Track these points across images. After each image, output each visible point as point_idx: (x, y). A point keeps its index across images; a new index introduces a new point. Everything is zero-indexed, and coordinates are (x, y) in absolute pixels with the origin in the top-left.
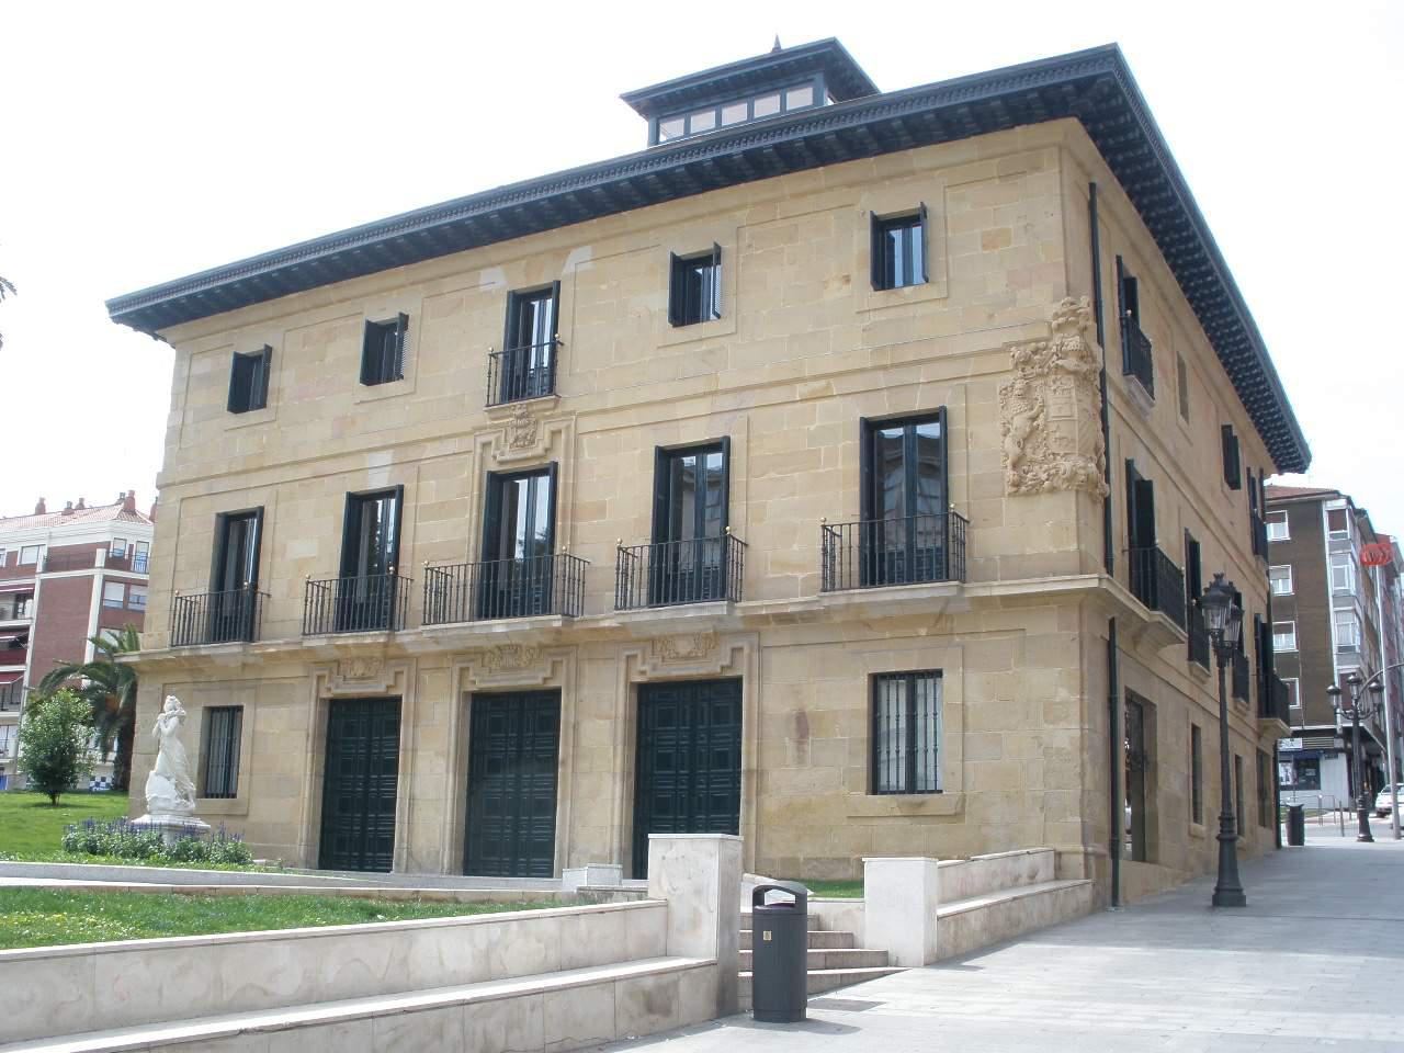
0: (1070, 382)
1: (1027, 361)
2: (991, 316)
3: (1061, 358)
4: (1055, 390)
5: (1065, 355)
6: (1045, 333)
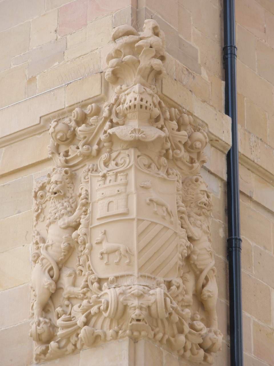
0: (128, 158)
1: (70, 138)
2: (32, 80)
3: (118, 124)
4: (104, 176)
5: (123, 119)
6: (93, 89)
